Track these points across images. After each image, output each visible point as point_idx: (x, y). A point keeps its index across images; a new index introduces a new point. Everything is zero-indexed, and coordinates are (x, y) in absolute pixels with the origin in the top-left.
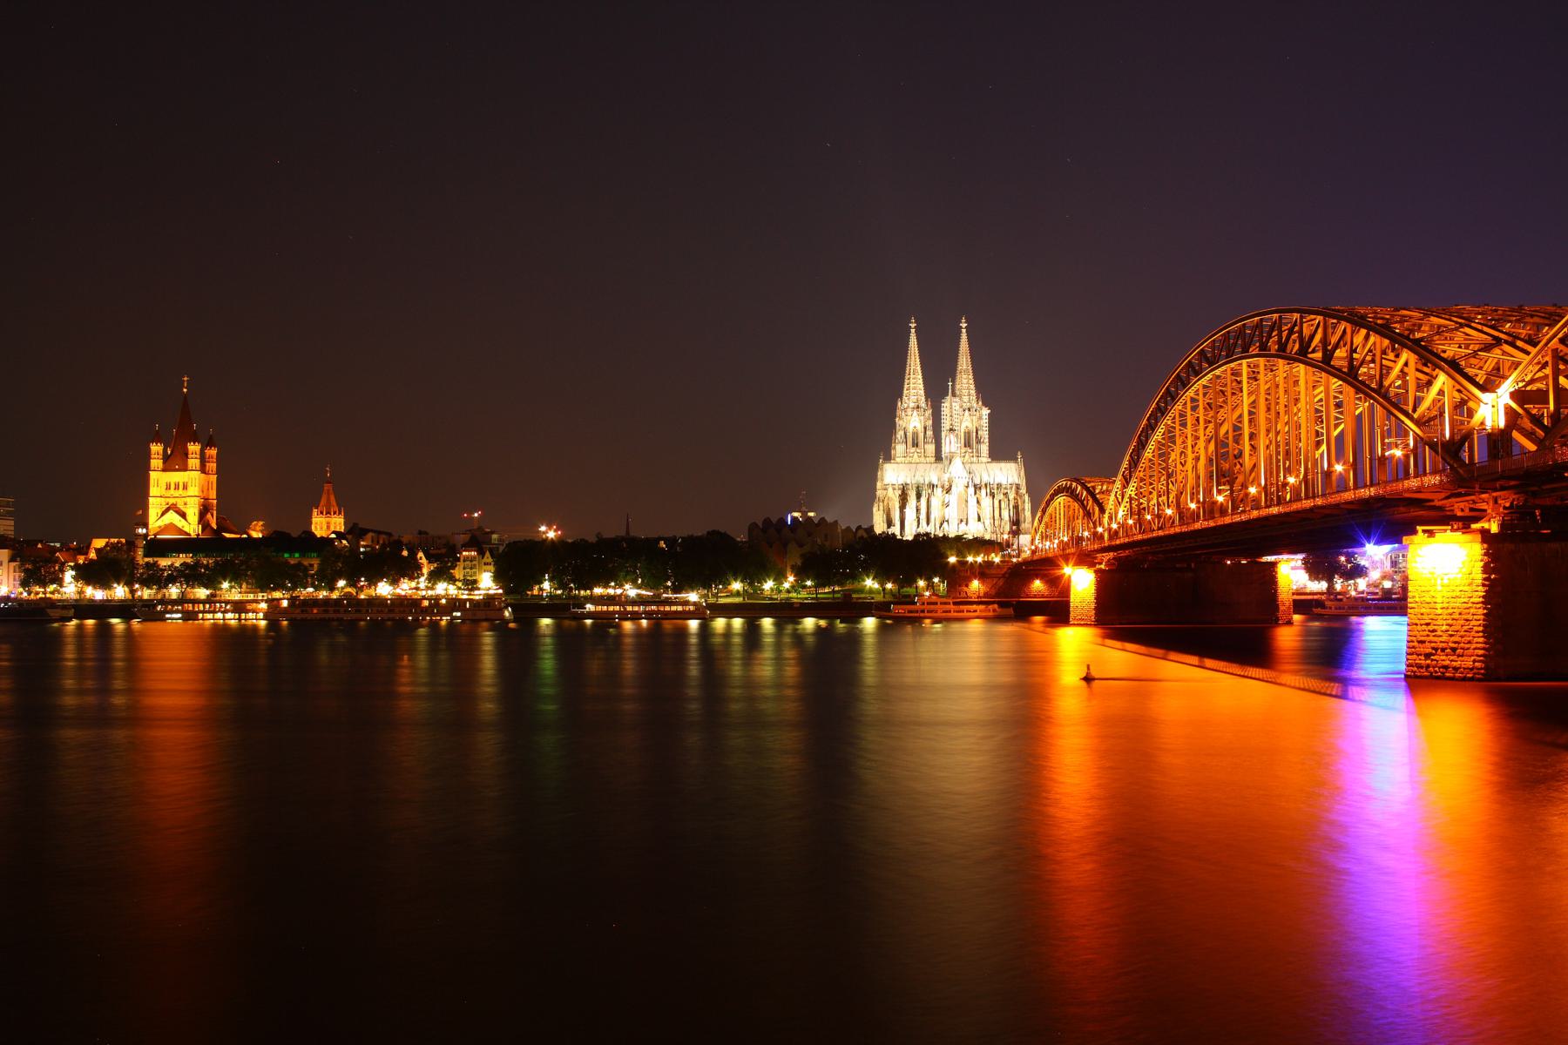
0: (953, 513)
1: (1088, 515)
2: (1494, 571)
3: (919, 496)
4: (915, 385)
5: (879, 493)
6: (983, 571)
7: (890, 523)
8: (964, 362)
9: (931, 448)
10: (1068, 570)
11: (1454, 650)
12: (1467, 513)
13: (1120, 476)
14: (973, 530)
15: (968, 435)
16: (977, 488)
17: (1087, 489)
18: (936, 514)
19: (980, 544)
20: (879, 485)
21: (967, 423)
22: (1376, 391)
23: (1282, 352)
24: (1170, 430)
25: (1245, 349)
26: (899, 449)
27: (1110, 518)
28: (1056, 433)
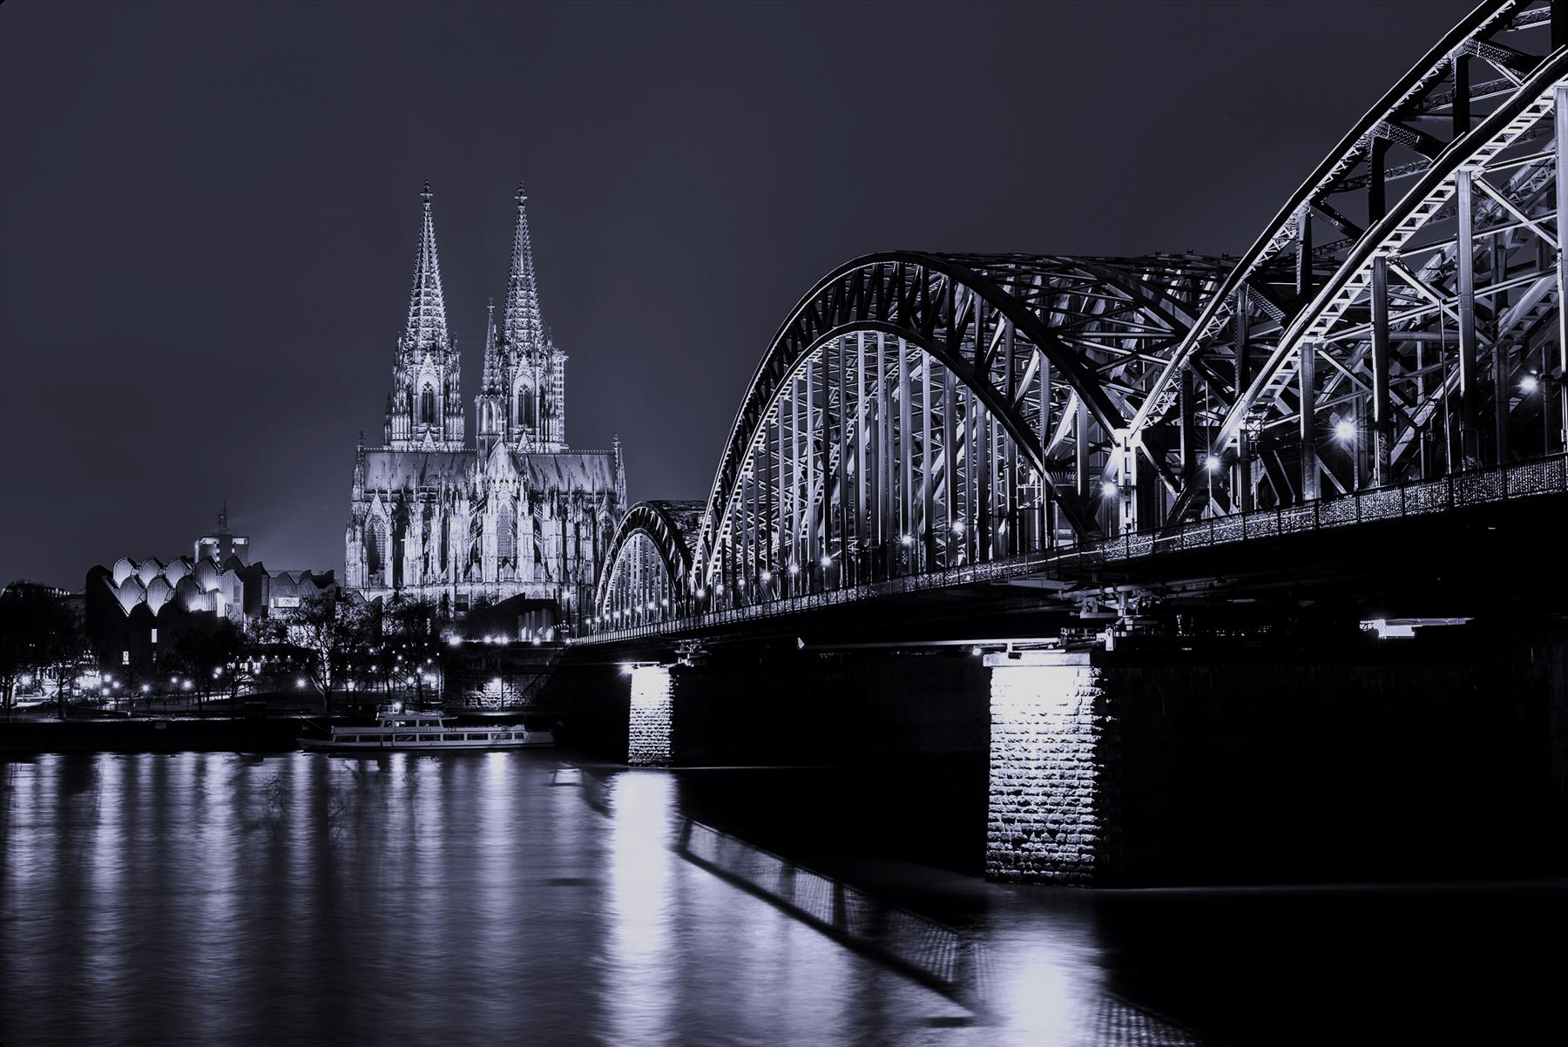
1: (671, 568)
2: (1110, 710)
3: (427, 515)
4: (431, 311)
5: (356, 506)
6: (511, 663)
7: (374, 564)
8: (522, 268)
9: (457, 424)
10: (626, 668)
11: (1053, 833)
13: (710, 507)
15: (527, 398)
17: (669, 522)
18: (459, 547)
20: (356, 491)
21: (524, 378)
22: (1009, 410)
23: (901, 329)
24: (771, 433)
25: (862, 314)
26: (399, 424)
27: (698, 577)
28: (663, 413)
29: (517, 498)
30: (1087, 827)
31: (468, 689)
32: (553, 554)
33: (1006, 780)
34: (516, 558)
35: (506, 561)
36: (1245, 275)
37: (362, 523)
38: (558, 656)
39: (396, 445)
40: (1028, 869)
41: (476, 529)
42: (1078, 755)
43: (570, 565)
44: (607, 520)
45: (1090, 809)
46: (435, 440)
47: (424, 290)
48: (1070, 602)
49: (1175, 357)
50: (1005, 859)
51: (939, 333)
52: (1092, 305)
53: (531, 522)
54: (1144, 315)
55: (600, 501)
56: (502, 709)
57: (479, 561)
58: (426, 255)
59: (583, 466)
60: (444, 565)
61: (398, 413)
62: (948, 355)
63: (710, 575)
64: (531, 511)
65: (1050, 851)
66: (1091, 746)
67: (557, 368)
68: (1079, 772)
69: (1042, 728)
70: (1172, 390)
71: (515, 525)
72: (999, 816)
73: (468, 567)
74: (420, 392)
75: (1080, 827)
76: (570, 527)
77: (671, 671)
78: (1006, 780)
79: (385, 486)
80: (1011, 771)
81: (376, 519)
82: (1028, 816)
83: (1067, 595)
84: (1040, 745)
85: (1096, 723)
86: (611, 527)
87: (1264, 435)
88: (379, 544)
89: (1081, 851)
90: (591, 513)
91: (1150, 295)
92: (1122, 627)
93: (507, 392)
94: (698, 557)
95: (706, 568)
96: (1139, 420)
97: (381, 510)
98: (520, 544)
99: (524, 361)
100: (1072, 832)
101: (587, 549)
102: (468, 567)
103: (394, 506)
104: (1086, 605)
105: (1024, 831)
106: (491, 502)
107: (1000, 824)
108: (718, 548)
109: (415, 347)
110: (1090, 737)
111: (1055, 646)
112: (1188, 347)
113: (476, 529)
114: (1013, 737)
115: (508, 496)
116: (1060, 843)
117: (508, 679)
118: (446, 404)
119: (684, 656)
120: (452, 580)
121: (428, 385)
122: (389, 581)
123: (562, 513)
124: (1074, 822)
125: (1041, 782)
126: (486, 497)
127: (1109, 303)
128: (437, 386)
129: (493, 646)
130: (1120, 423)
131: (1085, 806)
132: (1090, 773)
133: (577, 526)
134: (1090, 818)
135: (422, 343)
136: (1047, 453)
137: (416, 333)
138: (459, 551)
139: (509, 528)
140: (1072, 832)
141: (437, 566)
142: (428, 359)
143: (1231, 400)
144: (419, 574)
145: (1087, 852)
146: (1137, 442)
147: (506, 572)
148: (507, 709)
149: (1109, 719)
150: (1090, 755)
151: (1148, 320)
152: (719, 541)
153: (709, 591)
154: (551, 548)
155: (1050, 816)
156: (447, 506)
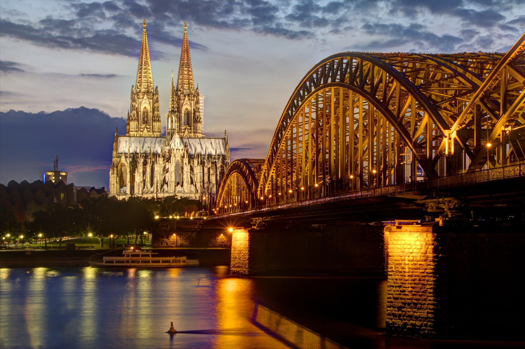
0: (171, 177)
1: (249, 187)
3: (145, 164)
5: (114, 159)
6: (180, 228)
7: (122, 184)
10: (230, 230)
11: (415, 304)
12: (434, 210)
14: (188, 191)
15: (188, 114)
16: (191, 157)
17: (249, 168)
18: (158, 178)
19: (186, 204)
20: (114, 153)
29: (183, 157)
30: (431, 302)
31: (162, 238)
32: (199, 180)
33: (395, 281)
34: (183, 182)
35: (178, 184)
36: (507, 61)
37: (117, 167)
38: (201, 224)
39: (132, 133)
40: (405, 320)
41: (166, 170)
42: (427, 271)
43: (206, 186)
44: (221, 166)
45: (432, 295)
46: (148, 131)
47: (143, 67)
48: (423, 205)
49: (472, 99)
50: (394, 315)
51: (367, 88)
52: (434, 76)
53: (189, 167)
54: (458, 80)
55: (219, 158)
56: (177, 246)
57: (167, 184)
58: (144, 52)
59: (211, 143)
60: (152, 185)
61: (132, 120)
62: (371, 96)
63: (266, 191)
64: (189, 162)
65: (414, 312)
66: (432, 267)
67: (200, 101)
68: (427, 278)
69: (411, 258)
70: (471, 113)
71: (183, 168)
72: (391, 296)
73: (162, 186)
74: (142, 111)
75: (428, 302)
76: (206, 170)
77: (249, 232)
78: (395, 281)
79: (127, 151)
80: (397, 277)
81: (123, 165)
82: (404, 297)
83: (423, 201)
84: (411, 266)
85: (434, 257)
86: (223, 170)
87: (512, 132)
88: (124, 175)
89: (428, 313)
90: (215, 163)
91: (461, 70)
92: (447, 216)
93: (179, 111)
94: (261, 182)
95: (264, 188)
96: (455, 127)
97: (126, 162)
98: (185, 176)
99: (187, 98)
100: (424, 304)
101: (213, 179)
102: (162, 186)
103: (131, 159)
104: (431, 205)
105: (403, 303)
106: (173, 159)
107: (392, 300)
108: (270, 179)
109: (140, 92)
110: (431, 263)
111: (417, 223)
112: (479, 93)
113: (166, 170)
114: (397, 262)
115: (180, 156)
116: (418, 309)
117: (179, 234)
118: (153, 117)
119: (255, 225)
120: (155, 191)
121: (145, 108)
122: (128, 192)
123: (202, 163)
124: (425, 300)
125: (410, 282)
126: (170, 156)
127: (443, 75)
128: (149, 108)
129: (173, 219)
130: (448, 127)
131: (430, 293)
132: (432, 279)
133: (209, 169)
134: (432, 298)
135: (143, 90)
136: (414, 140)
137: (140, 85)
138: (158, 179)
139: (179, 169)
140: (424, 304)
141: (149, 185)
142: (145, 97)
143: (498, 117)
144: (141, 188)
145: (431, 313)
146: (454, 135)
147: (179, 188)
148: (179, 247)
149: (440, 255)
150: (432, 271)
151: (460, 82)
152: (270, 176)
153: (266, 197)
154: (198, 178)
155: (414, 297)
156: (153, 160)
